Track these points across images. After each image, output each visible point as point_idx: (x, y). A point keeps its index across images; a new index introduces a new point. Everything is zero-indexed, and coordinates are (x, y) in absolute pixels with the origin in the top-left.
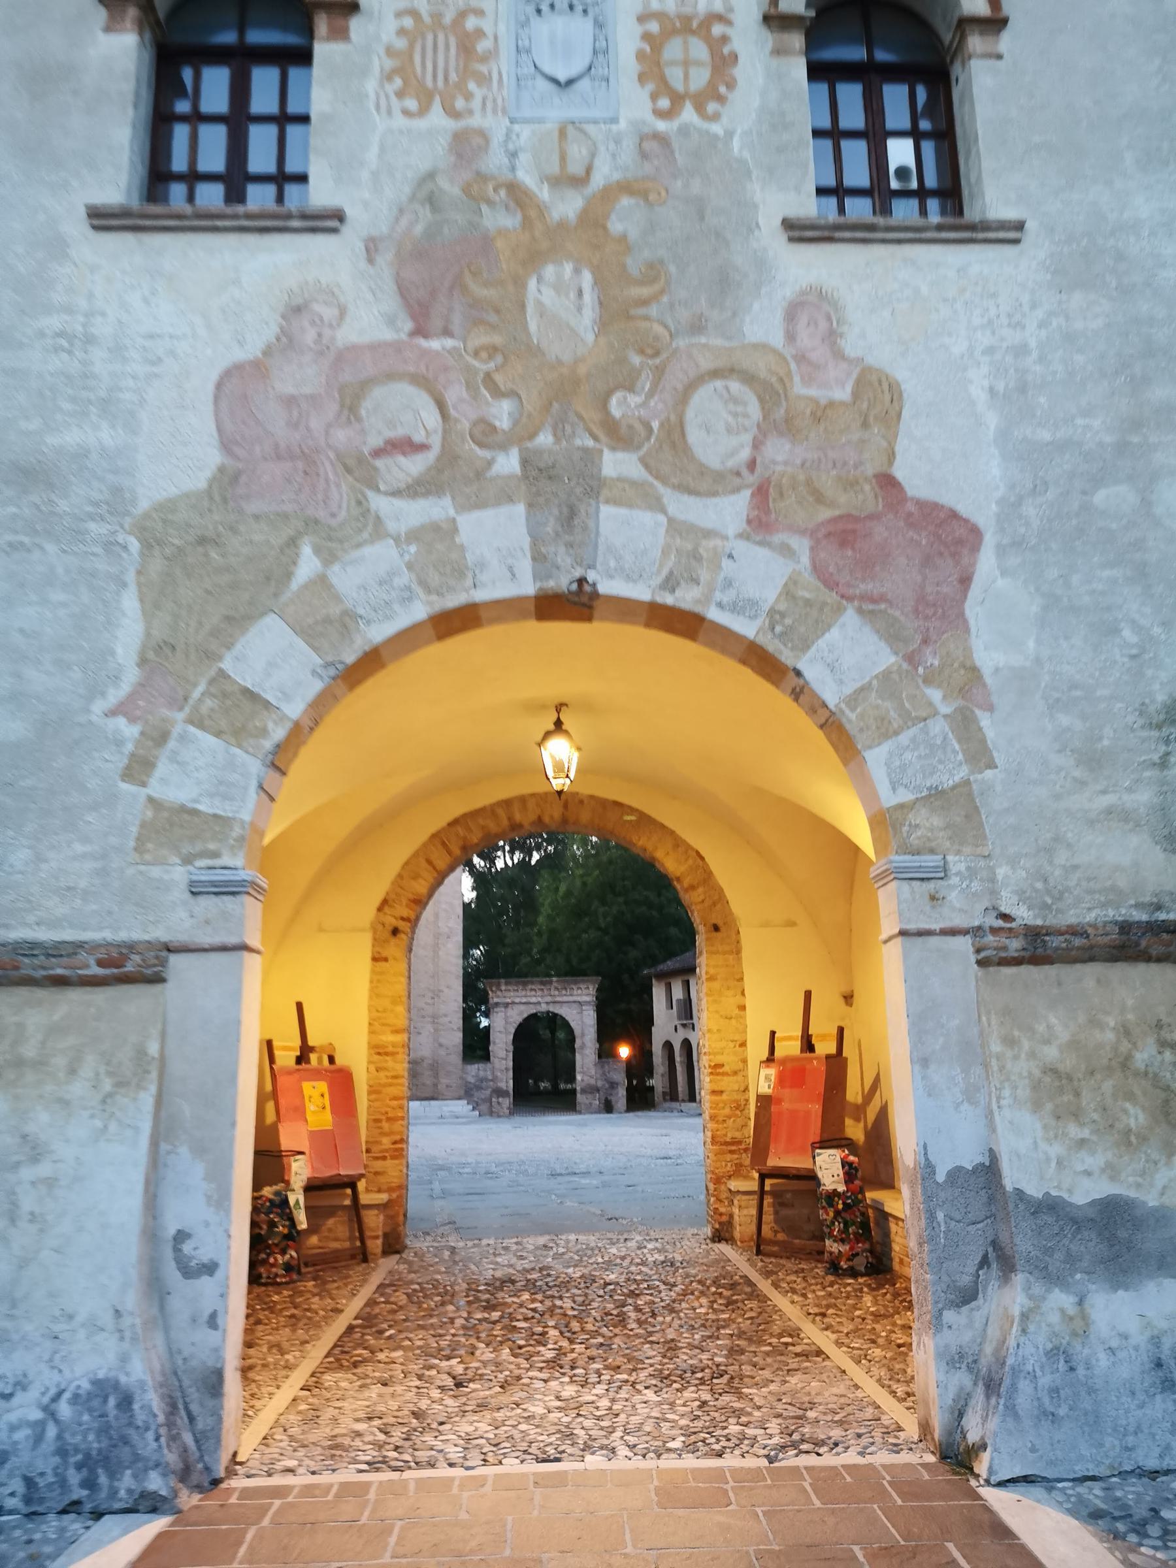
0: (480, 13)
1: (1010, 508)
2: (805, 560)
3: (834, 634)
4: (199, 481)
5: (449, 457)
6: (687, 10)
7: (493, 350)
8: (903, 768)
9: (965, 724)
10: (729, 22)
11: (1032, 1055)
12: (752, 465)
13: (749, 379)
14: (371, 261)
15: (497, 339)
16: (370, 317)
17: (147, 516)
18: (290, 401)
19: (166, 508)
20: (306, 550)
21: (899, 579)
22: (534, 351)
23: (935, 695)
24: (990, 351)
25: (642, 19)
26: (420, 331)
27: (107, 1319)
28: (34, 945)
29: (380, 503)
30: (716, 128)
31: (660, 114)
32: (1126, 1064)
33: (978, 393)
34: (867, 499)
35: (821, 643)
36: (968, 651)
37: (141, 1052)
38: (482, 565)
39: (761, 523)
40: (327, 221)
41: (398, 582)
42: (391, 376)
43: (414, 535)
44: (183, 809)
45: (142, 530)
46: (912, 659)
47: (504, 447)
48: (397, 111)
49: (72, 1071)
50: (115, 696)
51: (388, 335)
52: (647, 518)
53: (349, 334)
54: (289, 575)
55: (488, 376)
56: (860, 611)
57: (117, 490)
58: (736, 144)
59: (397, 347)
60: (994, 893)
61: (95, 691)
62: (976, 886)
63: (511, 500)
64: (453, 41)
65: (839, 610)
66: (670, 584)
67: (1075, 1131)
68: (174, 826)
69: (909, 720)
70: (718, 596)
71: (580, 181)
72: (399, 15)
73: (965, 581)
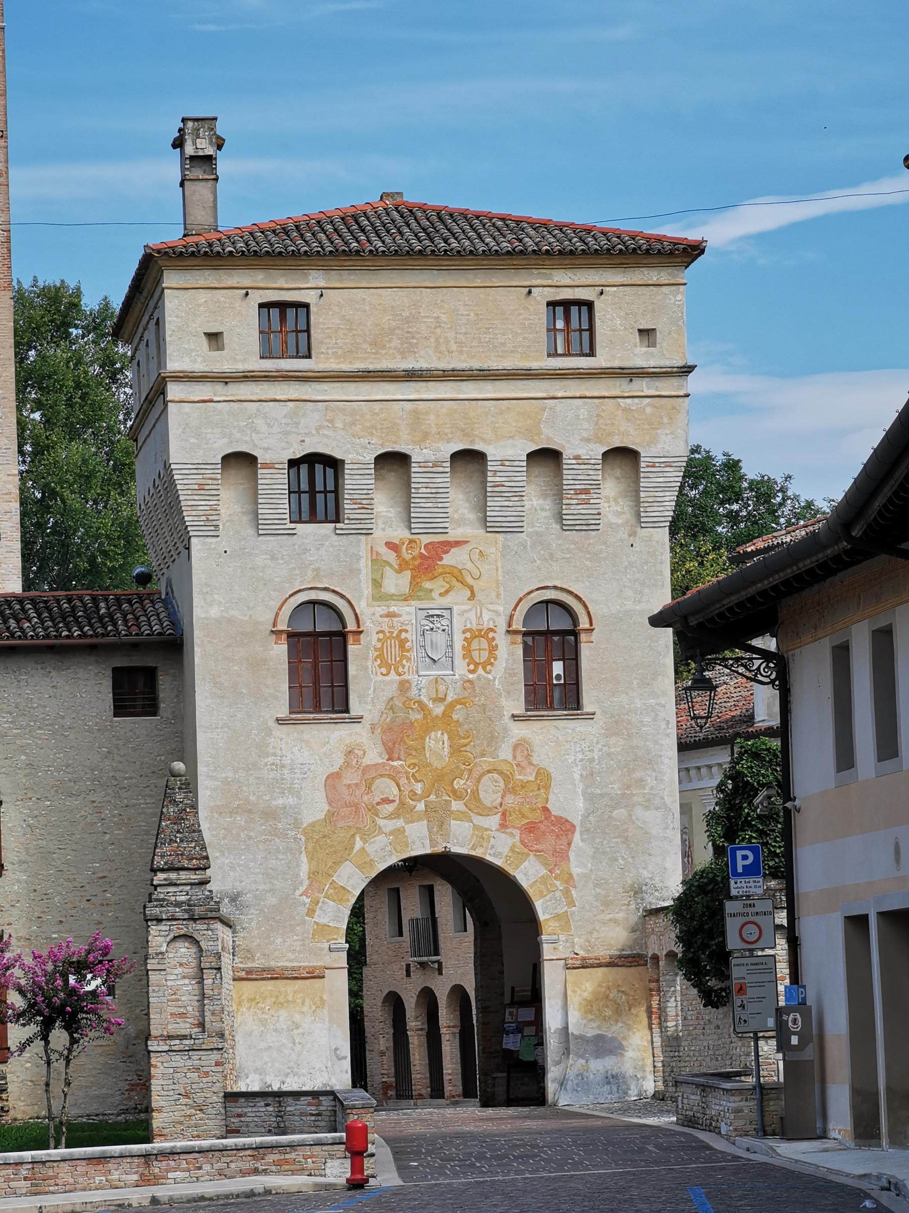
0: (407, 631)
1: (586, 817)
2: (518, 838)
3: (526, 863)
4: (321, 816)
5: (402, 804)
6: (480, 627)
7: (415, 765)
8: (547, 907)
9: (567, 893)
10: (495, 632)
11: (580, 995)
12: (501, 805)
13: (500, 773)
14: (373, 733)
15: (416, 761)
16: (374, 756)
17: (305, 829)
18: (349, 786)
19: (312, 825)
20: (358, 839)
21: (549, 843)
22: (429, 765)
23: (558, 883)
24: (581, 760)
25: (464, 632)
26: (389, 759)
27: (324, 1069)
28: (287, 967)
29: (381, 822)
30: (490, 676)
31: (470, 672)
32: (607, 997)
33: (577, 777)
34: (537, 816)
35: (522, 866)
36: (569, 869)
37: (321, 998)
38: (414, 842)
39: (503, 826)
40: (358, 720)
41: (388, 848)
42: (381, 776)
43: (391, 833)
44: (325, 925)
45: (305, 832)
46: (550, 871)
47: (419, 801)
48: (379, 674)
49: (303, 1004)
50: (302, 889)
51: (380, 761)
52: (467, 824)
53: (366, 761)
54: (353, 848)
55: (413, 775)
56: (535, 855)
57: (296, 819)
58: (497, 682)
59: (383, 765)
60: (573, 947)
61: (296, 889)
62: (568, 945)
63: (421, 819)
64: (397, 643)
65: (528, 855)
66: (474, 848)
67: (590, 1017)
68: (322, 930)
69: (549, 891)
70: (489, 851)
71: (443, 700)
72: (377, 633)
73: (569, 844)
